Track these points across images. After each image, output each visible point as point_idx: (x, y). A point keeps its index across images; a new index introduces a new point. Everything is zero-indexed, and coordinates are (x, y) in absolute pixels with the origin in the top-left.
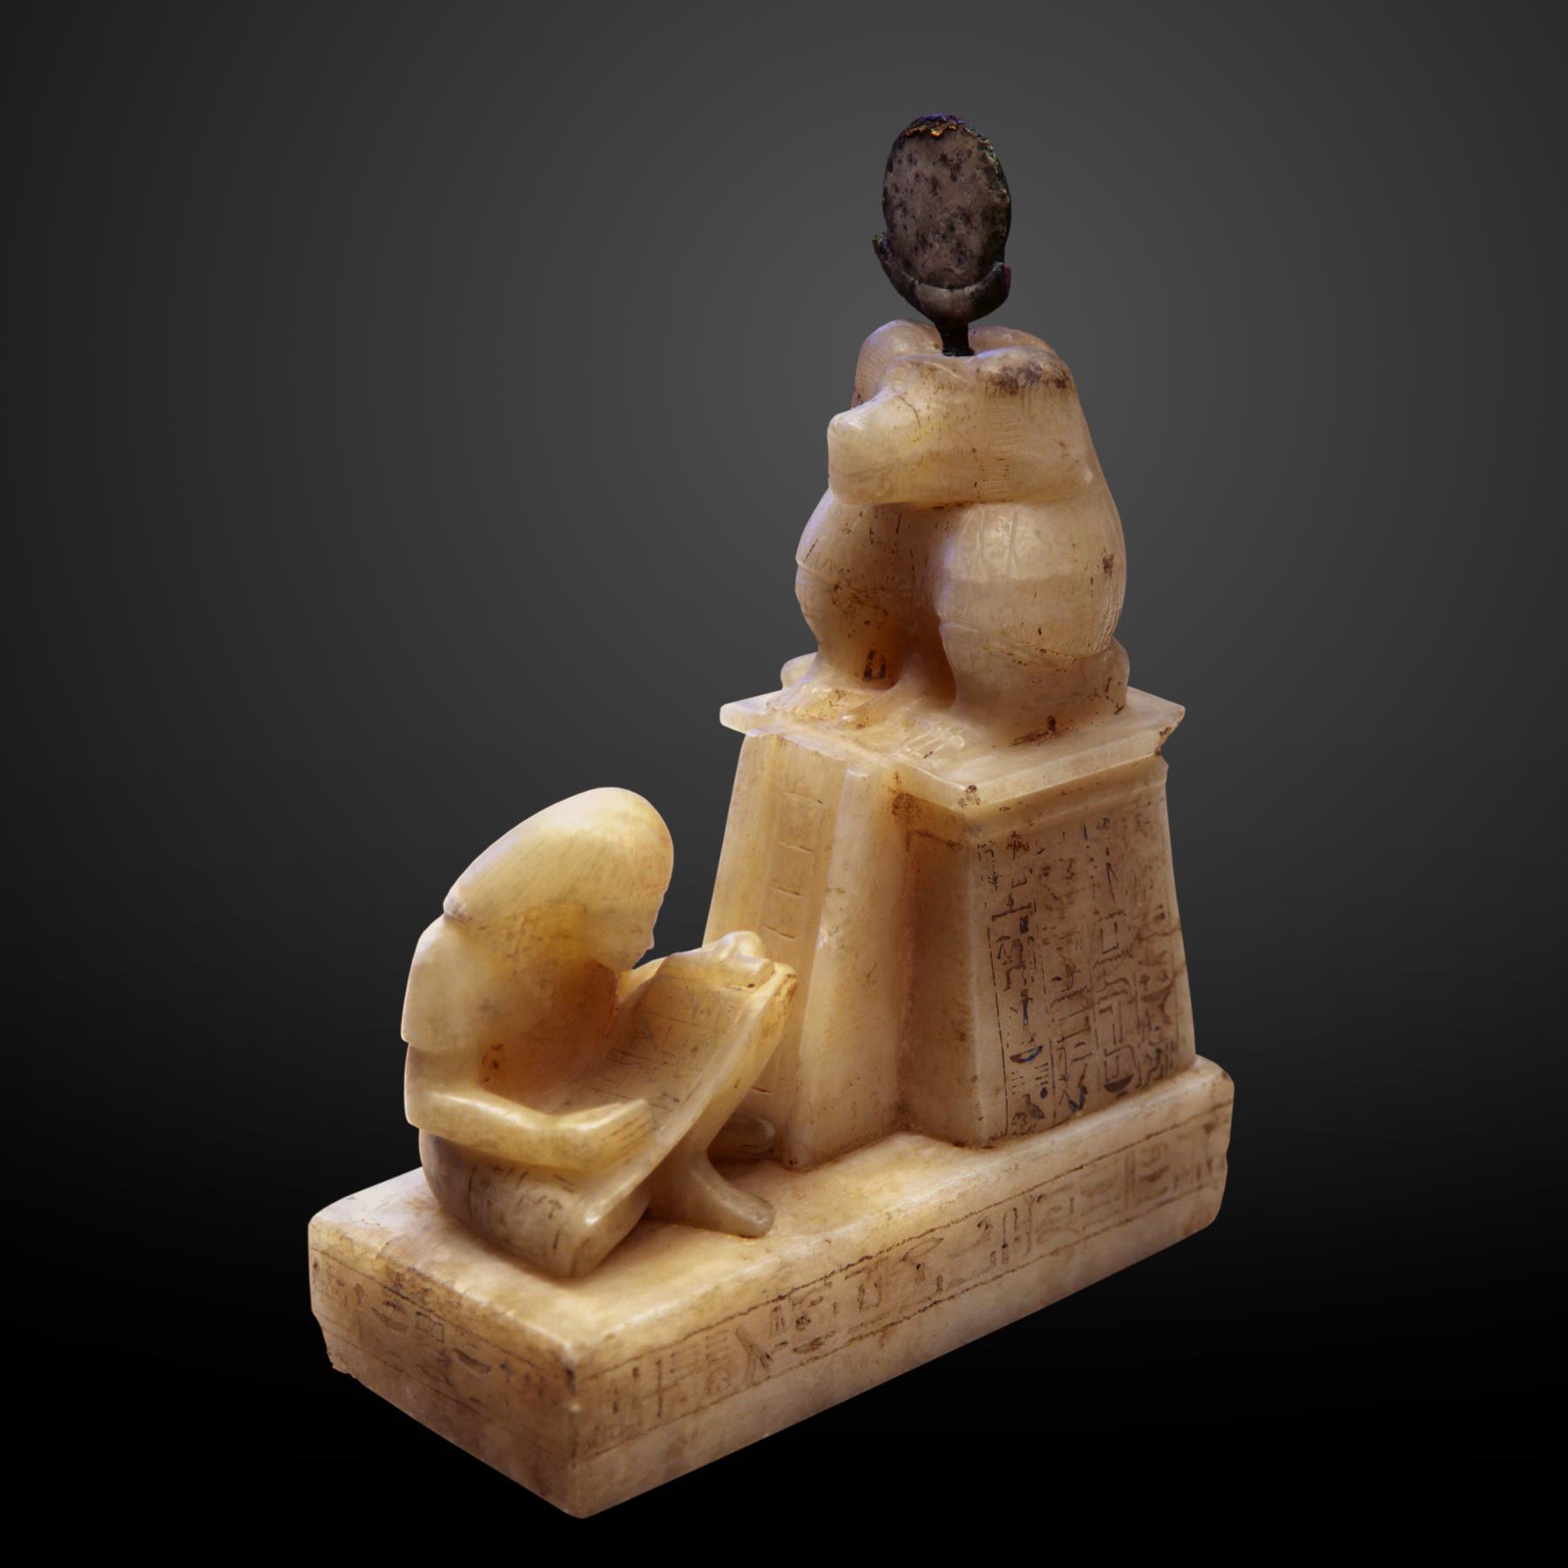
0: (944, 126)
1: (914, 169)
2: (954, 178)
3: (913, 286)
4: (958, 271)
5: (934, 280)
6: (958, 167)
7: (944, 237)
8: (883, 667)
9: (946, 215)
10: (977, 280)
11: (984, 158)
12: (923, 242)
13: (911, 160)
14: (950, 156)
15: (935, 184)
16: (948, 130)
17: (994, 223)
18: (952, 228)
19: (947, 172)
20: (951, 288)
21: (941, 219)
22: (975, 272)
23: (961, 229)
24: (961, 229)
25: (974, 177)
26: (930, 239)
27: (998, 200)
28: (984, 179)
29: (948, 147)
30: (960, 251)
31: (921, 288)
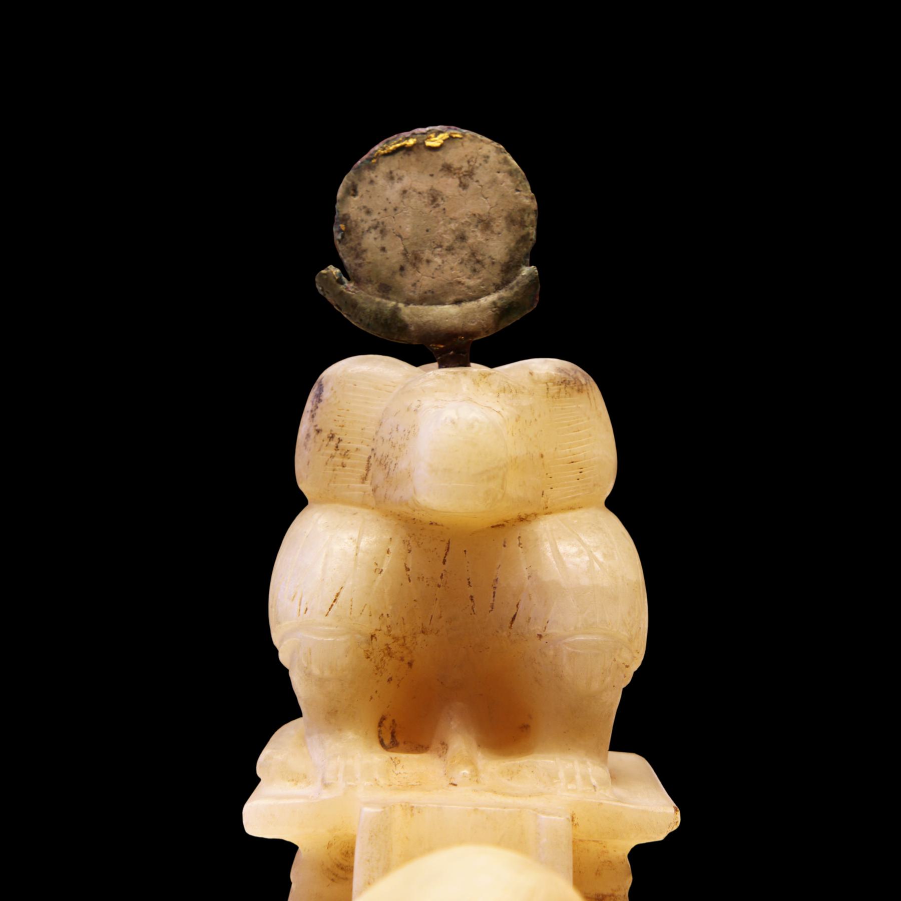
0: (445, 136)
1: (398, 186)
2: (464, 186)
3: (395, 310)
4: (471, 283)
5: (432, 298)
6: (470, 174)
7: (450, 249)
8: (393, 736)
9: (453, 226)
10: (498, 288)
11: (506, 161)
12: (414, 259)
13: (391, 177)
14: (456, 165)
15: (434, 198)
16: (451, 138)
17: (523, 224)
18: (462, 238)
19: (453, 182)
20: (457, 302)
21: (445, 232)
22: (497, 280)
23: (476, 236)
24: (476, 236)
25: (494, 181)
26: (427, 254)
27: (527, 202)
28: (508, 181)
29: (453, 156)
30: (475, 260)
31: (409, 313)
